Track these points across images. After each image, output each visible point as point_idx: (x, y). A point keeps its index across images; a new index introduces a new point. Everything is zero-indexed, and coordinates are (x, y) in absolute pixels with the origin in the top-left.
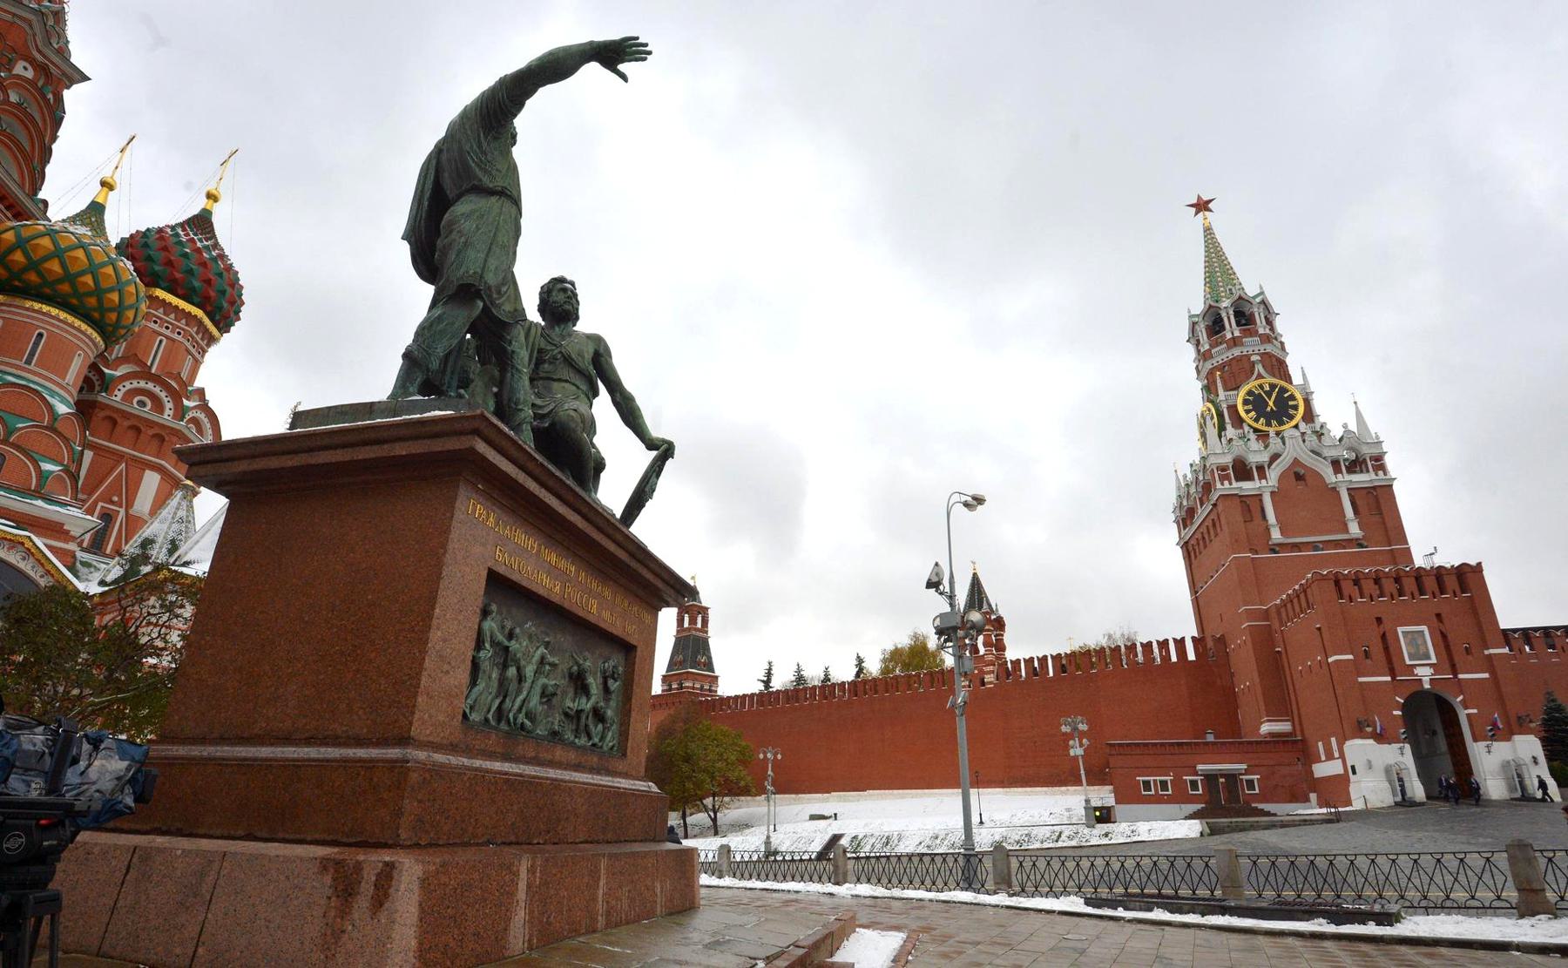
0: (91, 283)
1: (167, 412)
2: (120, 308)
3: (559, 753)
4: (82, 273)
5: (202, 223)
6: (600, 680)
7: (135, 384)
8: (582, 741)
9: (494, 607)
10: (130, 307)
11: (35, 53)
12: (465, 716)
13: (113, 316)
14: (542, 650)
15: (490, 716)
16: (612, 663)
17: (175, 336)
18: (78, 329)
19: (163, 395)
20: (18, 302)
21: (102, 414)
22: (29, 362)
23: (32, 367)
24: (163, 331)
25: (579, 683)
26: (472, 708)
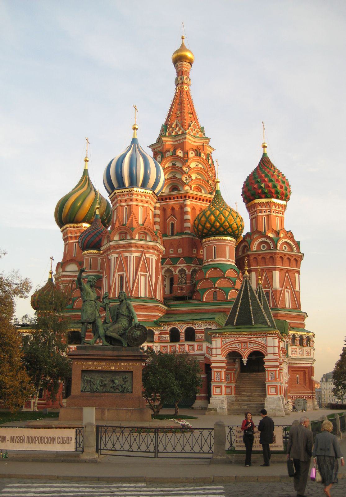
0: (218, 224)
1: (272, 246)
2: (230, 226)
3: (107, 394)
5: (265, 162)
6: (121, 379)
7: (259, 242)
8: (117, 391)
9: (86, 375)
12: (82, 391)
13: (230, 230)
16: (124, 377)
17: (268, 213)
19: (268, 241)
21: (252, 258)
22: (215, 258)
23: (216, 259)
24: (264, 214)
25: (113, 381)
26: (84, 390)
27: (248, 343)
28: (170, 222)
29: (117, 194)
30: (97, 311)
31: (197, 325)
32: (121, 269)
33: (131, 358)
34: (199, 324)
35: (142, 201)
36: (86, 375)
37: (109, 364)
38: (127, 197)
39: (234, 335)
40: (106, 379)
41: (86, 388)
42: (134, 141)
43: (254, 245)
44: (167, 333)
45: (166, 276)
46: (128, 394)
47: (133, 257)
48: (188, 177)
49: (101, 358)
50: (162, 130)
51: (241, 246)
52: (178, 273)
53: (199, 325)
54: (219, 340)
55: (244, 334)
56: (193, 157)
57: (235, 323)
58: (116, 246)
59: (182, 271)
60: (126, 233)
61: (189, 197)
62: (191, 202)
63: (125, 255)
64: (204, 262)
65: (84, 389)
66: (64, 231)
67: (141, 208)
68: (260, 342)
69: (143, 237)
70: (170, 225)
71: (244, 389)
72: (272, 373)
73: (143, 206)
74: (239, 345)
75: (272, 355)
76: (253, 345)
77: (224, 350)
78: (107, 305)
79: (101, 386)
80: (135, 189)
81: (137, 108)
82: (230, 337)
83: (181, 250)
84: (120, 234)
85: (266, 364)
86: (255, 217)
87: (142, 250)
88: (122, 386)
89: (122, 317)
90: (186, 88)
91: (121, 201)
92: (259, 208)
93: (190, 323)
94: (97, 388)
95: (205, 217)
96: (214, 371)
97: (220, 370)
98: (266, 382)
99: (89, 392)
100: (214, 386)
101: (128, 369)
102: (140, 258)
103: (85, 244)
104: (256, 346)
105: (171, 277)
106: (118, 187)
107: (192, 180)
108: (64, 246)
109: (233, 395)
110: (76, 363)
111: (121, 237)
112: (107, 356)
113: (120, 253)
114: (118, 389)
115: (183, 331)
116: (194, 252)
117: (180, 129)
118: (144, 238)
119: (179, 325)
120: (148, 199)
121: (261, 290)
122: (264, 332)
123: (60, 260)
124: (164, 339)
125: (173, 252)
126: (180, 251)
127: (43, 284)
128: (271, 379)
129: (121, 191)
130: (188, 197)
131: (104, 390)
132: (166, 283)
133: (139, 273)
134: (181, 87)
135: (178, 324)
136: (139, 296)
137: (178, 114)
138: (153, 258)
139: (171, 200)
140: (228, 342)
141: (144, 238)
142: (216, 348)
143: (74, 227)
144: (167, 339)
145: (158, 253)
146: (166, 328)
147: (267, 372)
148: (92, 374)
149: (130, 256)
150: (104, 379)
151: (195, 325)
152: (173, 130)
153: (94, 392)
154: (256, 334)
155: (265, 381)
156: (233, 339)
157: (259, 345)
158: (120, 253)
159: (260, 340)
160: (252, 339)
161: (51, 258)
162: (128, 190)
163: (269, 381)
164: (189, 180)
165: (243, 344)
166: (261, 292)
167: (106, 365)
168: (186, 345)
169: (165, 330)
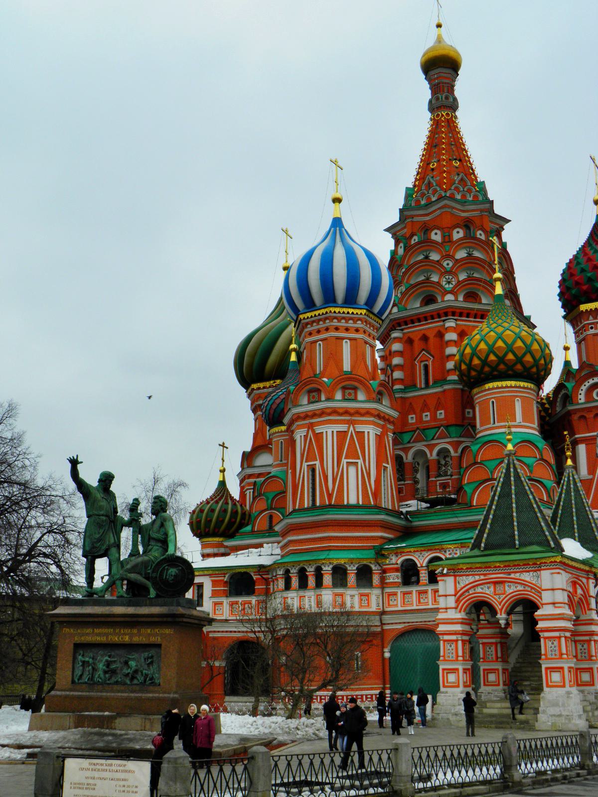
3: (115, 687)
4: (488, 355)
6: (143, 660)
8: (135, 682)
10: (525, 354)
11: (463, 214)
12: (73, 682)
13: (519, 367)
14: (107, 658)
15: (86, 680)
18: (507, 387)
20: (483, 388)
21: (575, 417)
23: (497, 424)
25: (126, 663)
26: (78, 680)
27: (506, 584)
28: (422, 364)
29: (303, 321)
30: (111, 535)
31: (448, 553)
32: (310, 457)
33: (156, 619)
34: (451, 550)
35: (347, 330)
36: (81, 652)
37: (120, 631)
38: (322, 325)
39: (477, 568)
40: (116, 659)
41: (81, 676)
42: (337, 223)
43: (580, 392)
44: (397, 570)
45: (418, 464)
46: (151, 688)
47: (333, 432)
48: (451, 277)
49: (103, 619)
50: (408, 196)
51: (560, 396)
52: (438, 454)
53: (451, 551)
54: (450, 580)
55: (495, 567)
56: (461, 239)
57: (483, 545)
58: (301, 415)
59: (443, 453)
60: (318, 391)
61: (454, 314)
62: (458, 322)
63: (318, 429)
64: (477, 431)
65: (77, 678)
66: (252, 395)
67: (346, 342)
68: (528, 579)
69: (350, 394)
70: (422, 368)
71: (529, 674)
72: (553, 643)
73: (350, 339)
74: (489, 588)
75: (551, 605)
76: (516, 587)
77: (461, 598)
78: (134, 523)
79: (105, 672)
80: (333, 310)
81: (340, 164)
82: (470, 573)
83: (443, 414)
84: (309, 392)
85: (541, 625)
86: (584, 339)
87: (347, 418)
88: (142, 673)
89: (152, 543)
90: (448, 114)
91: (310, 334)
92: (591, 320)
93: (435, 549)
94: (99, 677)
95: (472, 348)
96: (445, 641)
97: (454, 637)
98: (541, 662)
99: (86, 683)
100: (444, 670)
101: (153, 640)
102: (345, 433)
103: (271, 416)
104: (521, 589)
105: (427, 464)
106: (304, 309)
107: (459, 282)
108: (253, 421)
109: (501, 686)
111: (311, 397)
112: (114, 616)
113: (311, 426)
114: (136, 678)
115: (424, 565)
116: (467, 415)
117: (435, 192)
118: (352, 397)
119: (417, 553)
120: (359, 324)
121: (571, 478)
122: (534, 561)
123: (248, 448)
124: (391, 580)
125: (428, 418)
126: (441, 415)
127: (209, 490)
128: (552, 655)
129: (309, 315)
130: (451, 314)
131: (113, 680)
132: (419, 476)
133: (344, 461)
134: (438, 115)
135: (415, 551)
136: (346, 503)
137: (433, 165)
138: (371, 431)
139: (422, 323)
140: (467, 583)
141: (352, 397)
142: (446, 596)
143: (264, 388)
144: (396, 580)
145: (382, 423)
146: (394, 559)
147: (542, 640)
148: (93, 650)
149: (326, 432)
150: (113, 659)
151: (445, 552)
152: (423, 195)
153: (94, 683)
154: (518, 565)
155: (540, 658)
156: (477, 578)
157: (527, 588)
158: (311, 426)
159: (527, 577)
160: (512, 576)
161: (220, 445)
162: (321, 312)
163: (546, 659)
164: (454, 283)
165: (497, 586)
166: (572, 482)
167: (115, 634)
168: (430, 592)
169: (393, 564)
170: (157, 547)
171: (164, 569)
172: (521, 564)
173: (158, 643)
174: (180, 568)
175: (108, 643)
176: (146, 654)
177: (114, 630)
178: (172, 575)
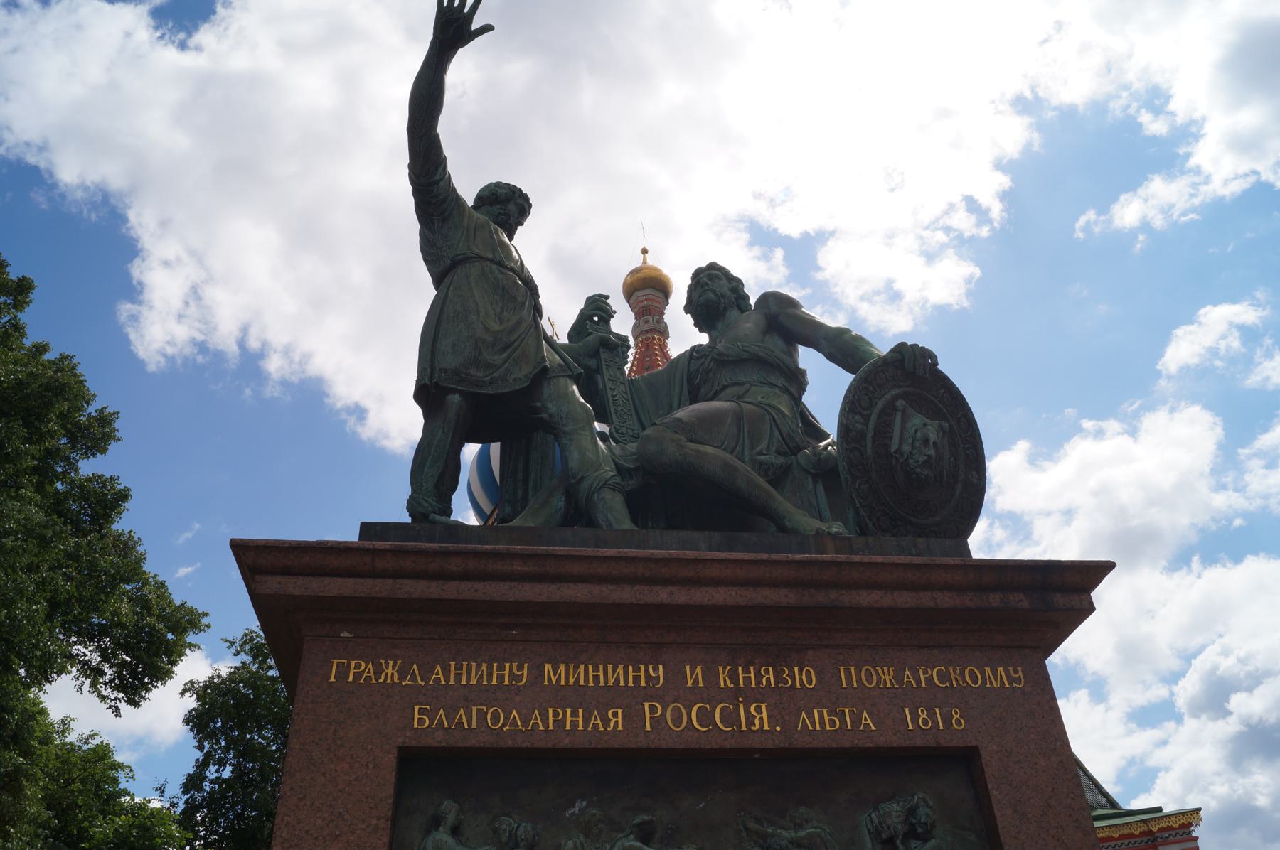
33: (946, 600)
36: (450, 809)
37: (711, 676)
49: (625, 595)
78: (604, 355)
101: (920, 724)
110: (342, 672)
122: (1144, 828)
167: (674, 692)
170: (766, 389)
171: (890, 409)
172: (1116, 836)
173: (956, 742)
174: (945, 424)
175: (641, 742)
176: (894, 811)
177: (675, 676)
178: (926, 441)
